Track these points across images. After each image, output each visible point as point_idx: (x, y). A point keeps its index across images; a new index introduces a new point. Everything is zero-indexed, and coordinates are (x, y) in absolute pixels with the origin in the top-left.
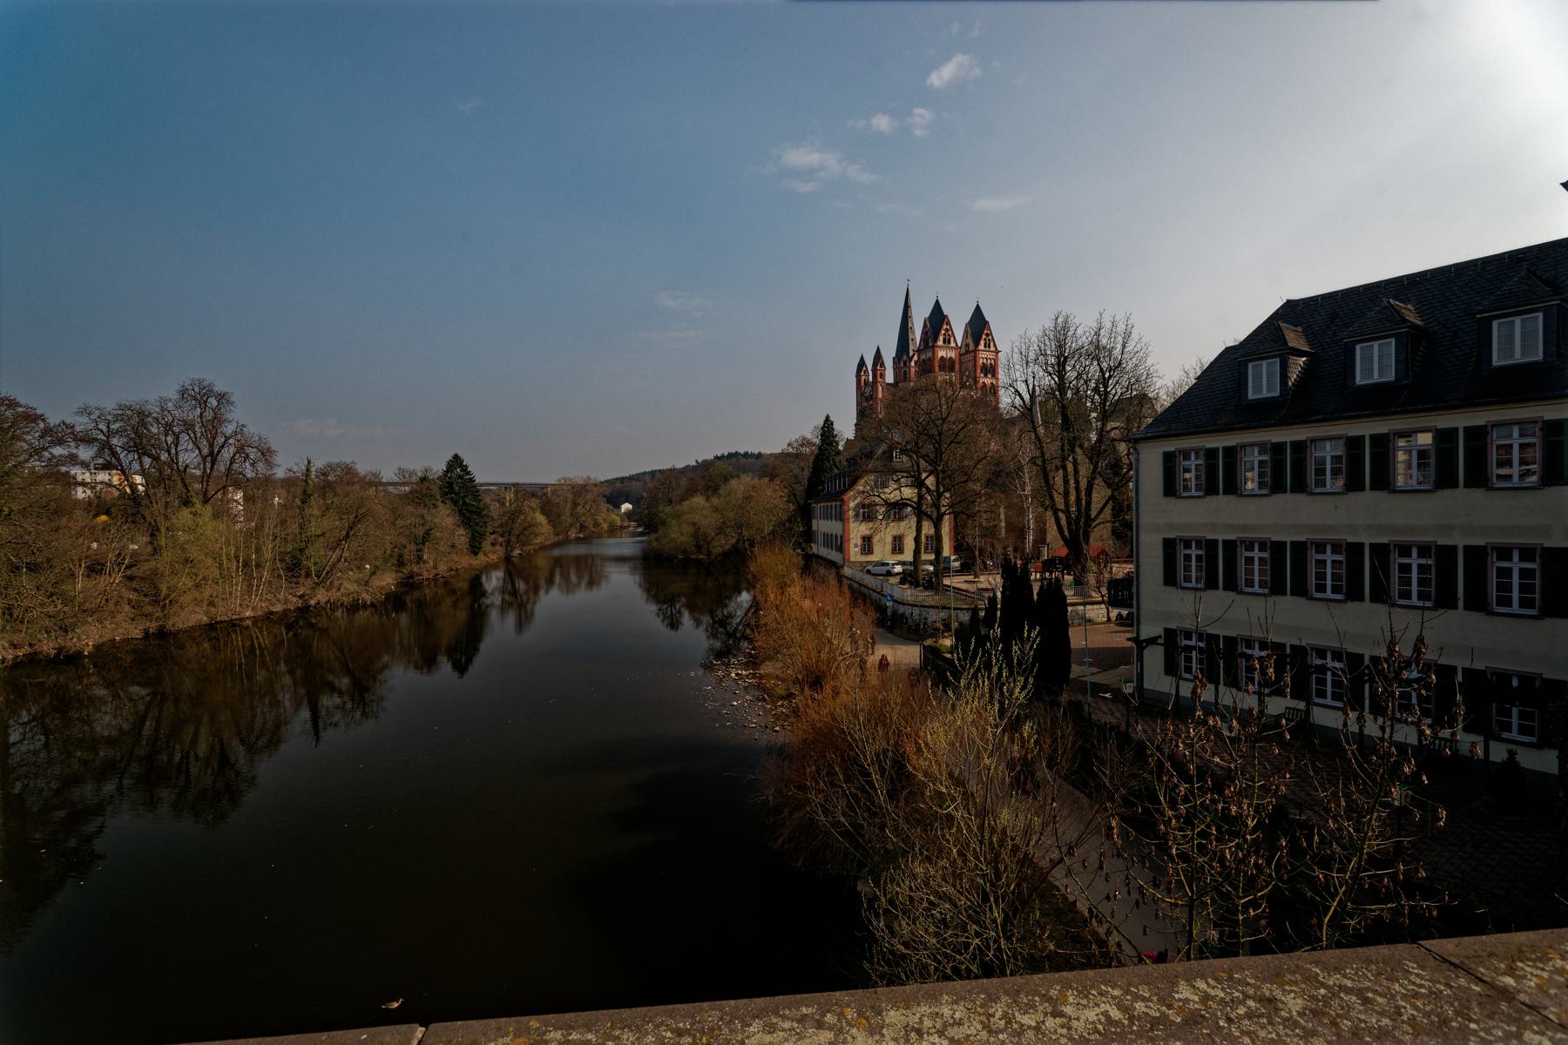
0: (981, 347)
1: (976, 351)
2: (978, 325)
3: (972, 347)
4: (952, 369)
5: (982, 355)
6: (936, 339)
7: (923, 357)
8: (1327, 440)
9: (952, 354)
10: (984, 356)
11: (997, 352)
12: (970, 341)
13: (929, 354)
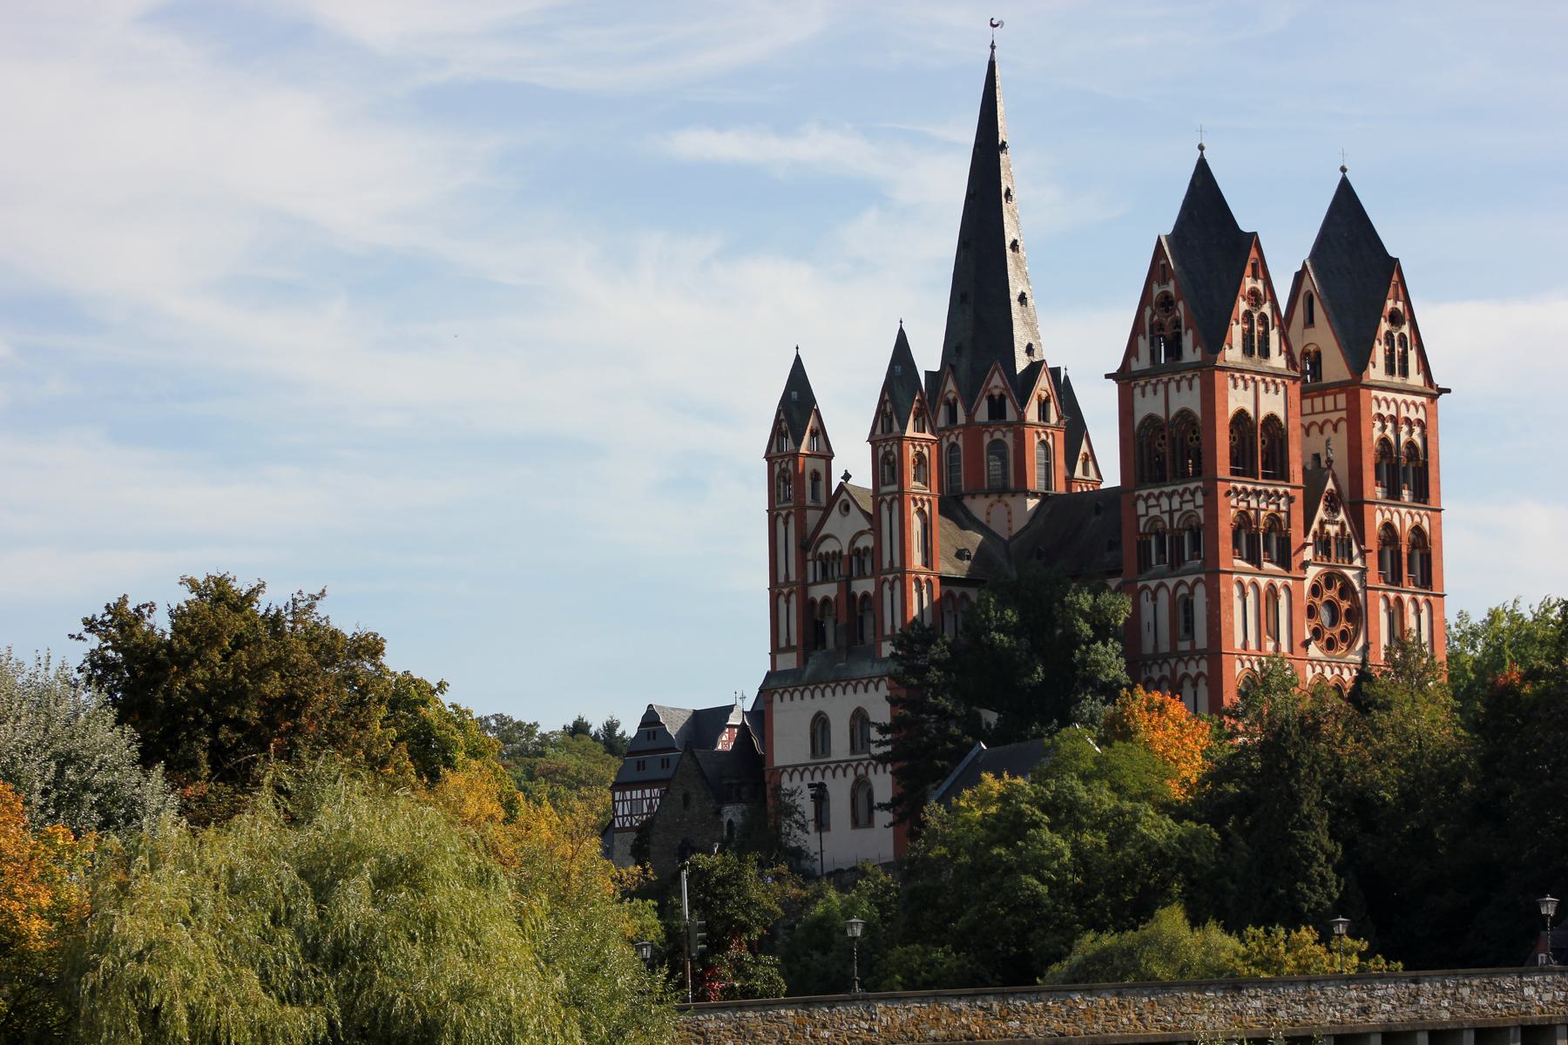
1: (1354, 387)
3: (1335, 367)
5: (1378, 404)
6: (1214, 340)
7: (1149, 405)
9: (1272, 404)
10: (1386, 405)
11: (1434, 393)
12: (1323, 337)
13: (1187, 399)
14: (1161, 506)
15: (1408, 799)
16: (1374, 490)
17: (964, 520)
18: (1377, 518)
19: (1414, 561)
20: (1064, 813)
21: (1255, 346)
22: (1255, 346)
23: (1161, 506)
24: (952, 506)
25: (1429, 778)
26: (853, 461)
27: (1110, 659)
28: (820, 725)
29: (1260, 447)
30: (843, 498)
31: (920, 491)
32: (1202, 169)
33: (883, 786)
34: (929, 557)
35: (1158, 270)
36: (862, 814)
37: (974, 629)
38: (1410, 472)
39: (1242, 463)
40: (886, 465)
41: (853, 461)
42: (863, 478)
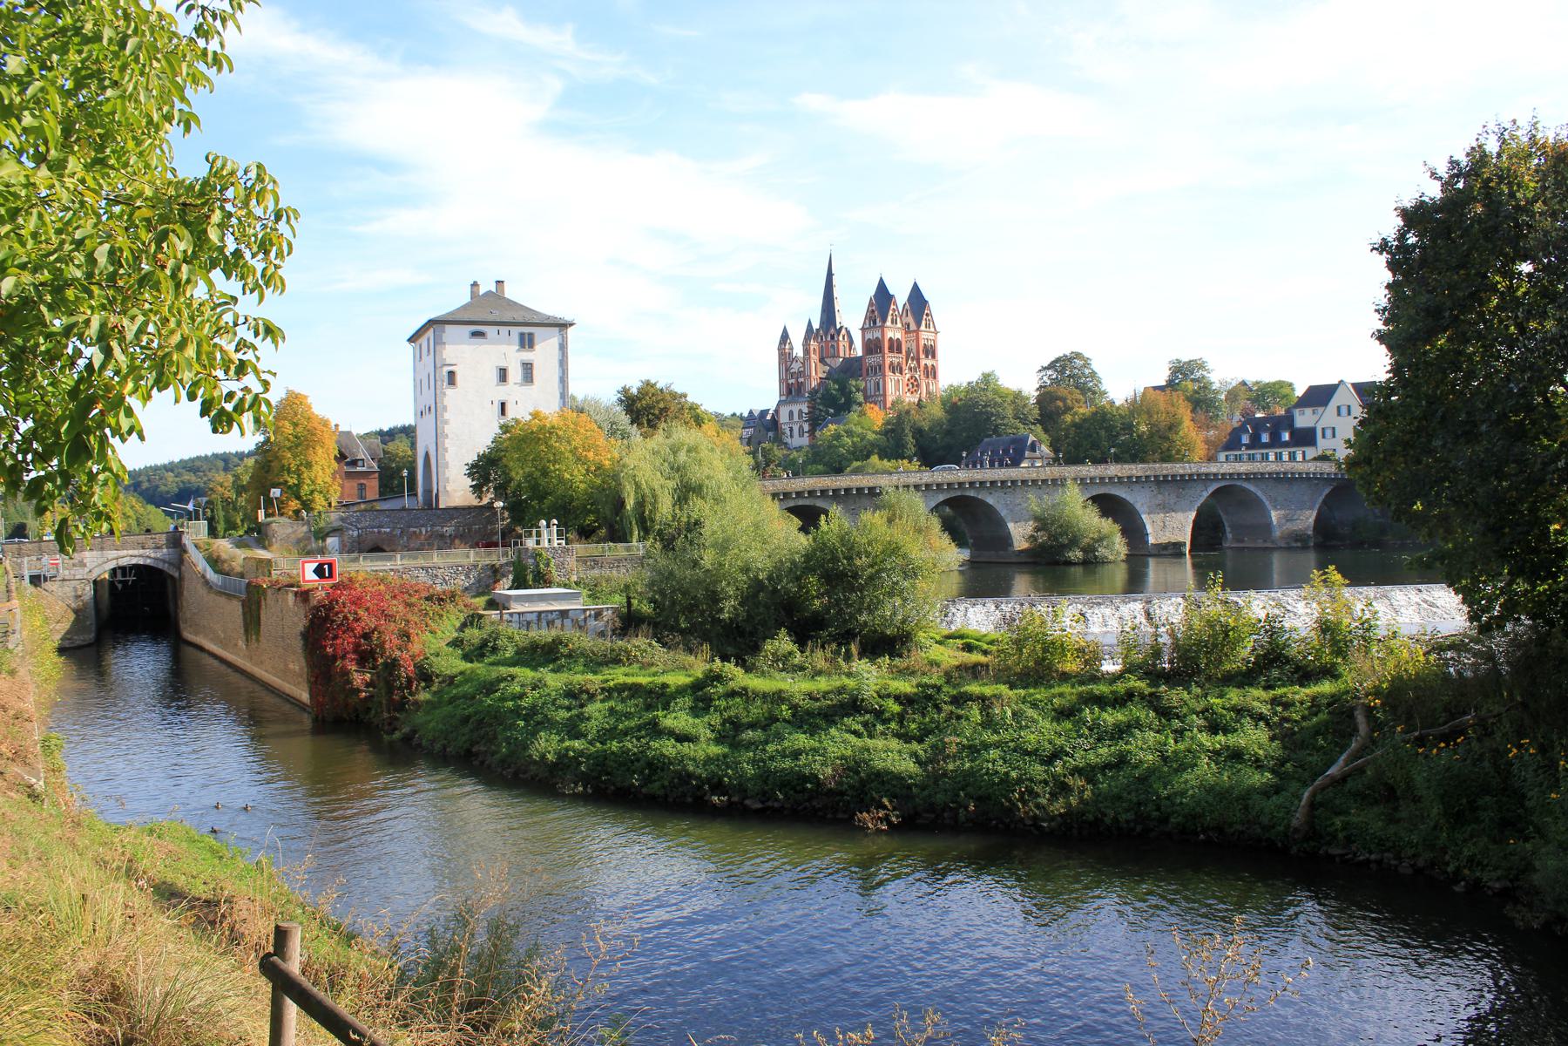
0: (923, 327)
1: (917, 331)
2: (918, 302)
3: (913, 327)
4: (899, 351)
5: (923, 335)
6: (884, 320)
7: (869, 336)
8: (1258, 452)
9: (898, 335)
10: (925, 336)
11: (936, 332)
12: (910, 319)
13: (878, 334)
14: (871, 360)
15: (931, 429)
16: (922, 356)
17: (826, 364)
18: (923, 362)
19: (932, 373)
20: (850, 433)
21: (894, 322)
22: (894, 322)
23: (871, 360)
24: (822, 360)
25: (938, 424)
26: (798, 351)
27: (860, 397)
28: (791, 413)
29: (895, 346)
30: (795, 359)
31: (815, 358)
32: (881, 281)
33: (806, 427)
34: (816, 374)
35: (871, 304)
36: (801, 434)
37: (827, 390)
38: (931, 351)
39: (891, 349)
40: (806, 351)
41: (798, 351)
42: (801, 354)
